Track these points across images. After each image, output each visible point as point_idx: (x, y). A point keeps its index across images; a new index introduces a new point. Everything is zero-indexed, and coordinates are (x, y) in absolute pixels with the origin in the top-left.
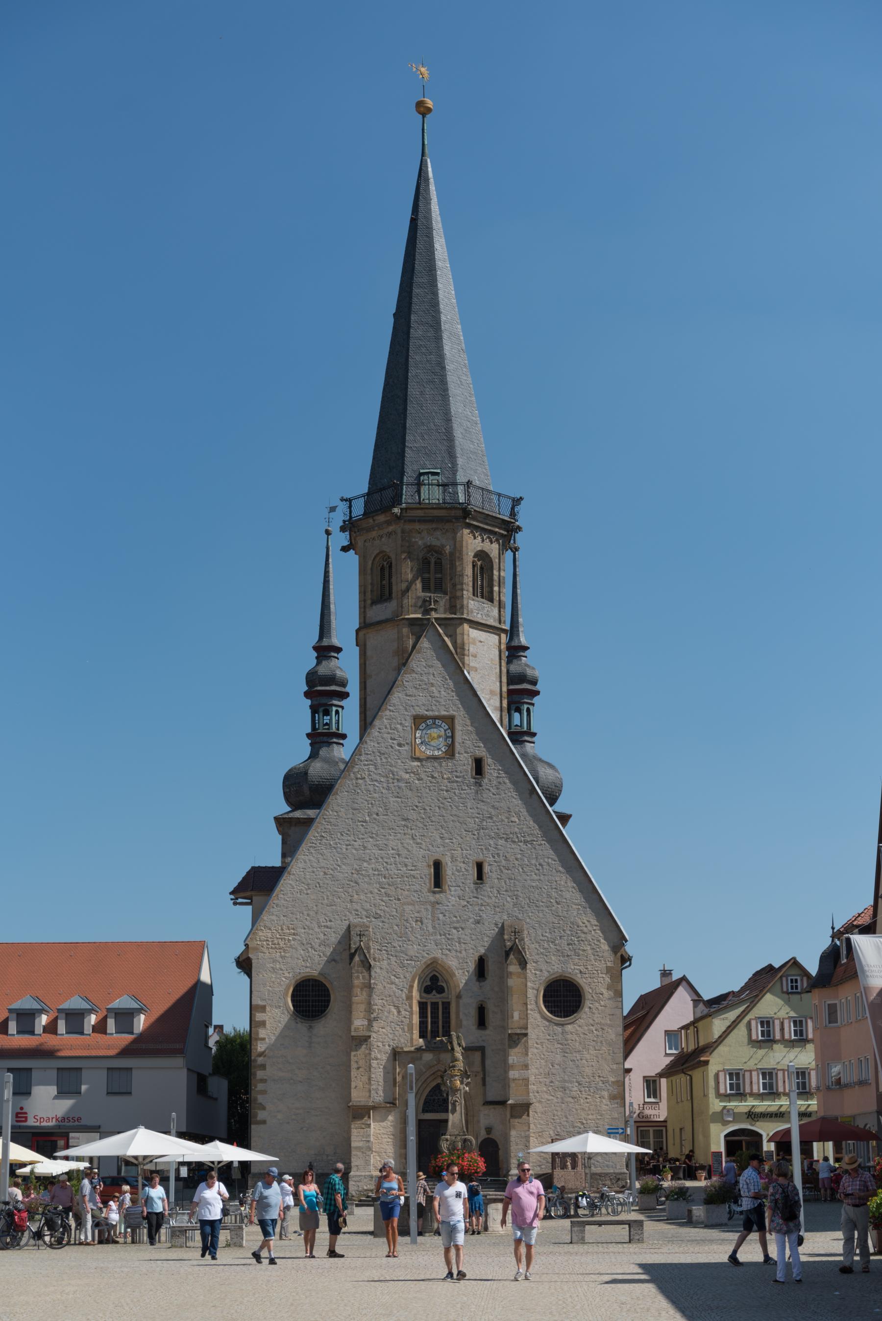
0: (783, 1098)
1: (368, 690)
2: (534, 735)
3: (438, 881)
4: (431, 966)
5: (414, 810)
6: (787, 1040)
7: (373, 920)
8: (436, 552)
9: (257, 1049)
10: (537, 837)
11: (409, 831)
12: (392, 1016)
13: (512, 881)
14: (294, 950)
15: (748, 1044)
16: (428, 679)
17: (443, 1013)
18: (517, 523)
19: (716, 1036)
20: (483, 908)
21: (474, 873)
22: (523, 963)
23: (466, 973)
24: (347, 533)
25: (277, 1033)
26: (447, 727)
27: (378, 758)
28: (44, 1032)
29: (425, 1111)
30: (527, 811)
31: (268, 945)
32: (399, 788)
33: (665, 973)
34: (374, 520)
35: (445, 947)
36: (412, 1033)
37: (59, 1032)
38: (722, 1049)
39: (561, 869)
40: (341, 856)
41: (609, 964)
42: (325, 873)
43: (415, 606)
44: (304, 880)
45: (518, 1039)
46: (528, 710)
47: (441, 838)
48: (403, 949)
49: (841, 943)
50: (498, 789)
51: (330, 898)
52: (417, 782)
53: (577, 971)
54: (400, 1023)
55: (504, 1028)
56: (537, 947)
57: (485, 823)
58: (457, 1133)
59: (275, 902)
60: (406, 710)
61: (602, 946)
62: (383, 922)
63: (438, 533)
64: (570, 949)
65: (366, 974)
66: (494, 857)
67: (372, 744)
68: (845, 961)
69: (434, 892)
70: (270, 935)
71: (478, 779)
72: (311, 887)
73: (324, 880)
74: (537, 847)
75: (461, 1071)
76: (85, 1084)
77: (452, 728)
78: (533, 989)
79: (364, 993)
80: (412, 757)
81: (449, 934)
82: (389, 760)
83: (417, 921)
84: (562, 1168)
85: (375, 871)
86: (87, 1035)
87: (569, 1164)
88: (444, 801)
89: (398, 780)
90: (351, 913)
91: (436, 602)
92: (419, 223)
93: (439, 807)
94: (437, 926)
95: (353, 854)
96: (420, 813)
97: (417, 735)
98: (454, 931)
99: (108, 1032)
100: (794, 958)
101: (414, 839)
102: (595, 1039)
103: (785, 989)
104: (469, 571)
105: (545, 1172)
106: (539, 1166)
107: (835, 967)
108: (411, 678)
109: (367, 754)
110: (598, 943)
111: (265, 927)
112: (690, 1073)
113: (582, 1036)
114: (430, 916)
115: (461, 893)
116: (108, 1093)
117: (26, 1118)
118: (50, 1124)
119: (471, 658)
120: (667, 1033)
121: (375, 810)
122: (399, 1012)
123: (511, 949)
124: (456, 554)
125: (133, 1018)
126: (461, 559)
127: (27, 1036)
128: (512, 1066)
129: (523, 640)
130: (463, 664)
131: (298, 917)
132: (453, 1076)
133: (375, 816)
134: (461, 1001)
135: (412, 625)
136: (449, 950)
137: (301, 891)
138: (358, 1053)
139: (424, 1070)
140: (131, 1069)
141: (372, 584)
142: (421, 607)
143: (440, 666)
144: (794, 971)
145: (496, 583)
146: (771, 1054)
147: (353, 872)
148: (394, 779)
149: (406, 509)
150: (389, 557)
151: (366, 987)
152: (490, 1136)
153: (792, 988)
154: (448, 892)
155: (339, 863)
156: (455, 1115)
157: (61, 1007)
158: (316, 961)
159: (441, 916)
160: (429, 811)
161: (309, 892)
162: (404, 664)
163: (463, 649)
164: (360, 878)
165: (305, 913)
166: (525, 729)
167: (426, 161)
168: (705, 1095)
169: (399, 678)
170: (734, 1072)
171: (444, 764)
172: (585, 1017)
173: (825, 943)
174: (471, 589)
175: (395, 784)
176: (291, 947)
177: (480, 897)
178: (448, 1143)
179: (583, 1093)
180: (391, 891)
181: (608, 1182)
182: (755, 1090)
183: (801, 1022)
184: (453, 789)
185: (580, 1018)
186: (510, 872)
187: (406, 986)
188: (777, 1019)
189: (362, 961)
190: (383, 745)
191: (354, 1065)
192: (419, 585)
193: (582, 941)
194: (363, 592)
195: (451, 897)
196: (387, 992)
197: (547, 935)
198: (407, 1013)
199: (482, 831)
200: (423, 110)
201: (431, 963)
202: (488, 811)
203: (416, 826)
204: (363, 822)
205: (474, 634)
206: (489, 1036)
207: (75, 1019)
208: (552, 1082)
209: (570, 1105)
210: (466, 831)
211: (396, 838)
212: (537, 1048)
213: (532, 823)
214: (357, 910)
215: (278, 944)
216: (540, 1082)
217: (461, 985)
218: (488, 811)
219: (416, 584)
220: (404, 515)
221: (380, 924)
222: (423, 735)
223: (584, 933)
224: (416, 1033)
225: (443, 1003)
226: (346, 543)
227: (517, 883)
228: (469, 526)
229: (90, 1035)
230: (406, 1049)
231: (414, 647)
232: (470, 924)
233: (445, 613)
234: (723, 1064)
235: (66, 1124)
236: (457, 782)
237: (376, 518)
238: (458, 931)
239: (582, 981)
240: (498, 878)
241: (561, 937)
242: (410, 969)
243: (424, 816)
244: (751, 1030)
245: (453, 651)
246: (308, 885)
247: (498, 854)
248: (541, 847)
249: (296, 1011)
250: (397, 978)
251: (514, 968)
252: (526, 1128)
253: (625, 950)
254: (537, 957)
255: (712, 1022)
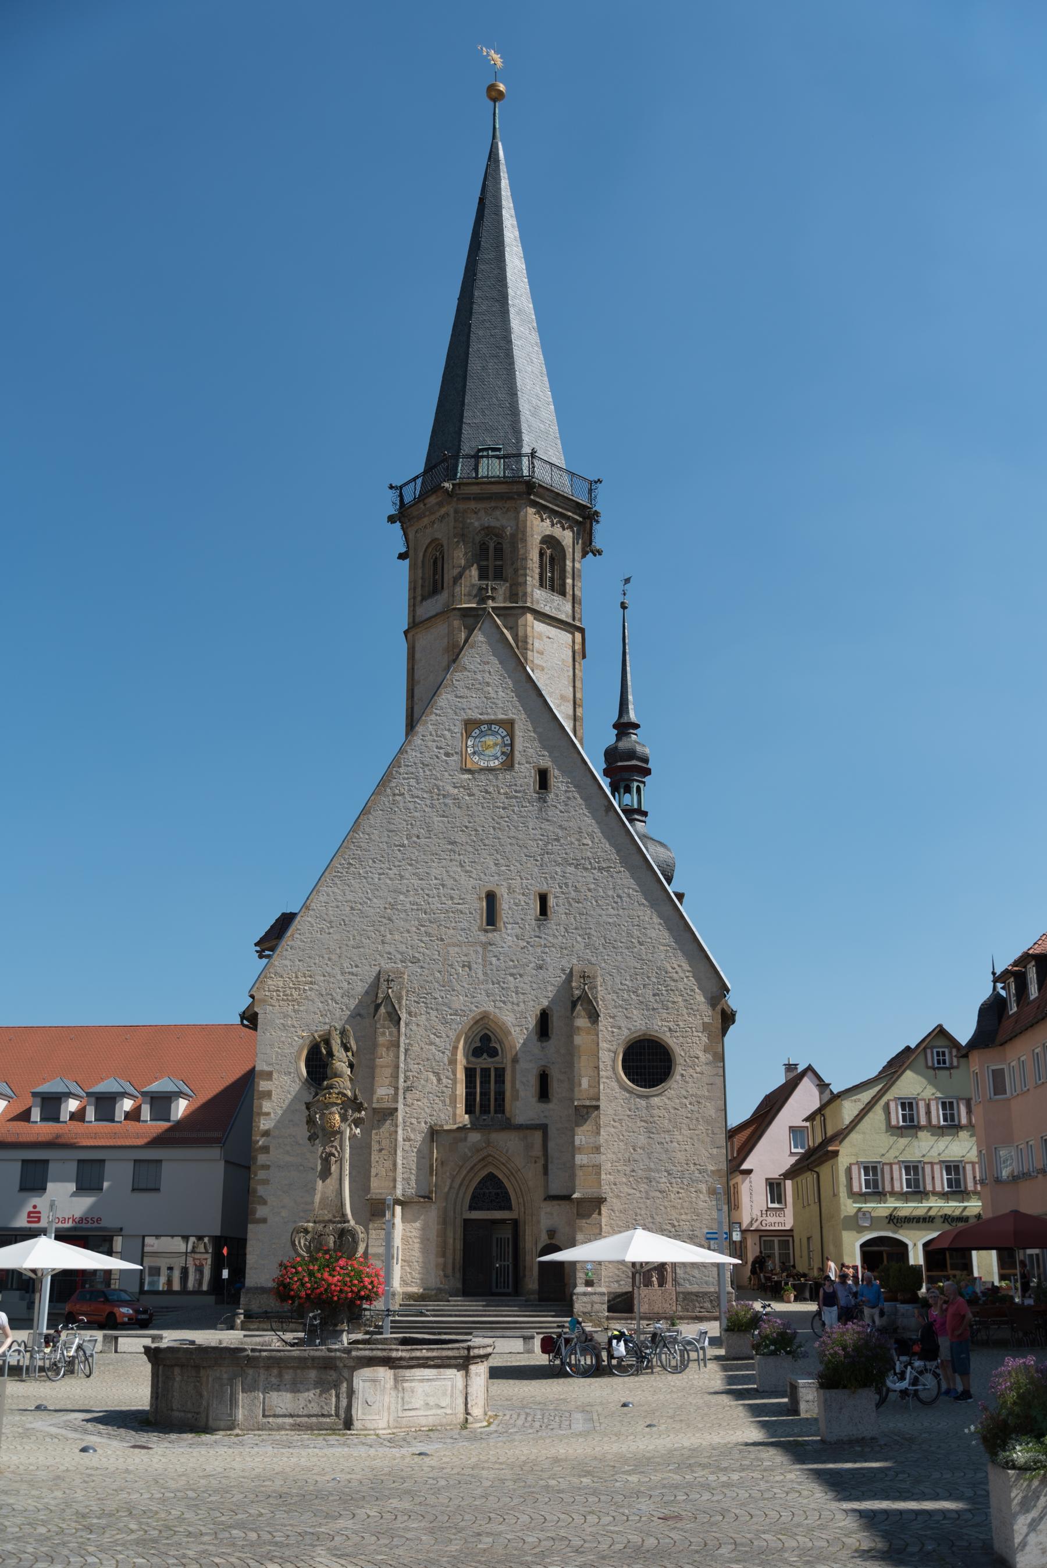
0: (932, 1198)
1: (416, 698)
2: (645, 814)
3: (492, 918)
4: (481, 1023)
5: (462, 831)
6: (934, 1126)
7: (410, 964)
8: (496, 536)
9: (259, 1127)
10: (615, 863)
11: (457, 856)
12: (430, 1086)
13: (584, 917)
14: (310, 1003)
15: (887, 1132)
16: (483, 677)
17: (496, 1083)
18: (594, 509)
19: (847, 1122)
20: (547, 950)
21: (536, 906)
22: (594, 1016)
23: (525, 1031)
24: (398, 524)
25: (284, 1106)
26: (505, 733)
27: (421, 770)
28: (70, 1119)
29: (472, 1208)
30: (602, 833)
31: (279, 996)
32: (446, 805)
33: (790, 1067)
34: (425, 505)
35: (498, 998)
36: (455, 1107)
37: (87, 1119)
38: (854, 1137)
39: (645, 902)
40: (372, 887)
41: (706, 1020)
42: (352, 908)
43: (469, 595)
44: (325, 916)
45: (587, 1113)
46: (638, 789)
47: (496, 864)
48: (445, 1000)
49: (1009, 993)
50: (566, 805)
51: (357, 938)
52: (467, 798)
53: (666, 1029)
54: (440, 1095)
55: (572, 1100)
56: (615, 998)
57: (550, 847)
58: (329, 1217)
59: (289, 943)
60: (456, 714)
61: (697, 997)
62: (422, 967)
63: (498, 513)
64: (656, 1001)
65: (394, 1030)
66: (561, 887)
67: (414, 754)
68: (1015, 1009)
69: (486, 931)
70: (281, 984)
71: (542, 794)
72: (333, 924)
73: (351, 916)
74: (615, 875)
75: (344, 1095)
76: (107, 1181)
77: (512, 735)
78: (610, 1051)
79: (391, 1054)
80: (461, 769)
81: (504, 982)
82: (434, 772)
83: (464, 966)
84: (646, 1286)
85: (413, 905)
86: (118, 1122)
87: (654, 1279)
88: (499, 820)
89: (444, 796)
90: (382, 956)
91: (493, 589)
92: (487, 202)
93: (494, 828)
94: (489, 972)
95: (386, 884)
96: (471, 835)
97: (470, 743)
98: (511, 979)
99: (142, 1119)
100: (940, 1026)
101: (462, 866)
102: (689, 1115)
103: (930, 1064)
104: (534, 556)
105: (624, 1290)
106: (617, 1282)
107: (1000, 1021)
108: (462, 677)
109: (408, 766)
110: (692, 993)
111: (276, 974)
112: (816, 1169)
113: (672, 1111)
114: (480, 960)
115: (519, 931)
116: (133, 1190)
117: (39, 1218)
118: (66, 1225)
119: (535, 654)
120: (792, 1129)
121: (415, 832)
122: (439, 1080)
123: (579, 998)
124: (520, 535)
125: (171, 1103)
126: (524, 540)
127: (50, 1124)
128: (579, 1148)
129: (633, 716)
130: (526, 659)
131: (317, 961)
132: (329, 1105)
133: (415, 839)
134: (517, 1067)
135: (464, 616)
136: (504, 1002)
137: (322, 930)
138: (381, 1130)
139: (470, 1154)
140: (161, 1161)
141: (422, 578)
142: (475, 596)
143: (497, 662)
144: (941, 1042)
145: (569, 575)
146: (915, 1143)
147: (387, 906)
148: (439, 795)
149: (459, 484)
150: (442, 546)
151: (393, 1045)
152: (553, 1242)
153: (939, 1063)
154: (503, 930)
155: (370, 895)
156: (328, 1181)
157: (91, 1090)
158: (338, 1016)
159: (494, 960)
160: (481, 832)
161: (331, 931)
162: (454, 661)
163: (526, 642)
164: (394, 914)
165: (326, 956)
166: (636, 806)
167: (497, 144)
168: (835, 1195)
169: (448, 676)
170: (870, 1165)
171: (501, 776)
172: (676, 1087)
173: (984, 991)
174: (537, 577)
175: (441, 801)
176: (307, 998)
177: (543, 936)
178: (309, 1237)
179: (675, 1185)
180: (433, 929)
181: (708, 1305)
182: (897, 1188)
183: (951, 1103)
184: (511, 806)
185: (670, 1088)
186: (580, 905)
187: (448, 1047)
188: (921, 1100)
189: (389, 1014)
190: (427, 754)
191: (375, 1147)
192: (474, 572)
193: (672, 990)
194: (413, 589)
195: (507, 937)
196: (424, 1055)
197: (627, 982)
198: (450, 1081)
199: (546, 856)
200: (494, 95)
201: (482, 1019)
202: (554, 832)
203: (465, 850)
204: (400, 846)
205: (540, 627)
206: (554, 1112)
207: (105, 1103)
208: (633, 1171)
209: (657, 1201)
210: (526, 856)
211: (440, 865)
212: (614, 1127)
213: (607, 846)
214: (390, 953)
215: (292, 995)
216: (618, 1171)
217: (518, 1046)
218: (554, 832)
219: (470, 571)
220: (458, 492)
221: (419, 970)
222: (476, 743)
223: (674, 980)
224: (461, 1107)
225: (496, 1069)
226: (403, 550)
227: (590, 919)
228: (534, 504)
229: (121, 1122)
230: (446, 1128)
231: (466, 641)
232: (530, 969)
233: (504, 602)
234: (856, 1155)
235: (84, 1225)
236: (516, 797)
237: (426, 501)
238: (515, 979)
239: (672, 1042)
240: (566, 913)
241: (644, 986)
242: (454, 1026)
243: (475, 839)
244: (890, 1113)
245: (514, 645)
246: (331, 922)
247: (566, 885)
248: (619, 875)
249: (312, 1079)
250: (438, 1037)
251: (582, 1022)
252: (598, 1231)
253: (726, 1002)
254: (614, 1011)
255: (842, 1105)
